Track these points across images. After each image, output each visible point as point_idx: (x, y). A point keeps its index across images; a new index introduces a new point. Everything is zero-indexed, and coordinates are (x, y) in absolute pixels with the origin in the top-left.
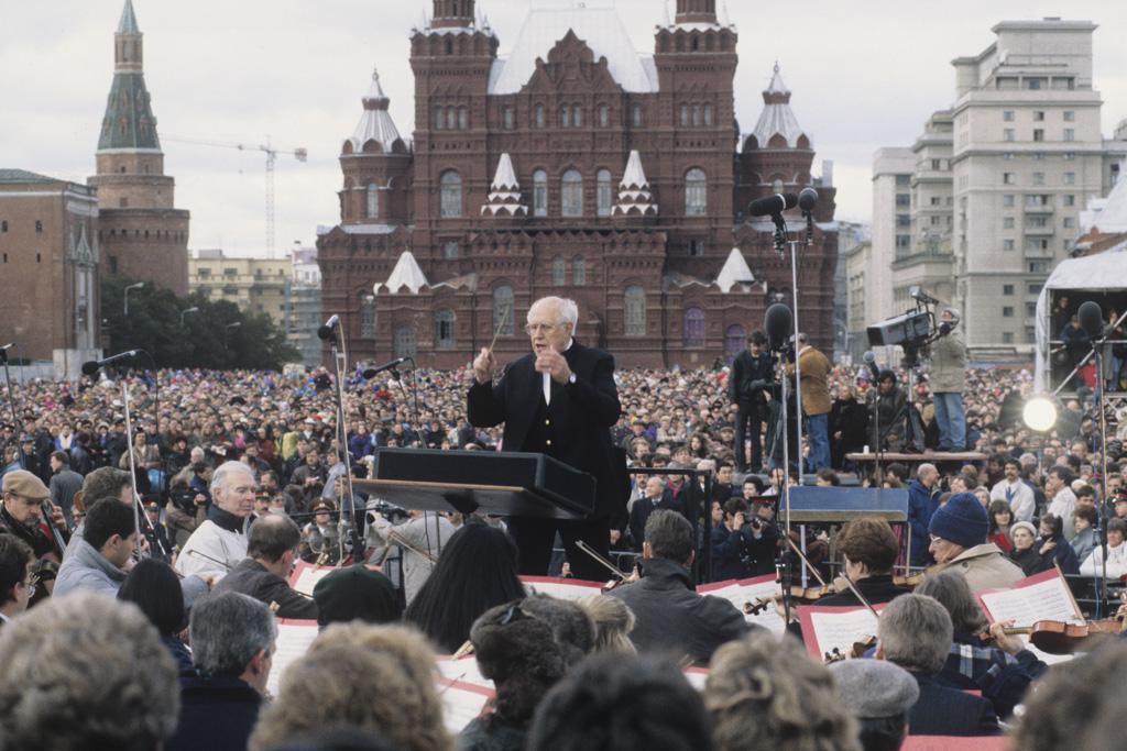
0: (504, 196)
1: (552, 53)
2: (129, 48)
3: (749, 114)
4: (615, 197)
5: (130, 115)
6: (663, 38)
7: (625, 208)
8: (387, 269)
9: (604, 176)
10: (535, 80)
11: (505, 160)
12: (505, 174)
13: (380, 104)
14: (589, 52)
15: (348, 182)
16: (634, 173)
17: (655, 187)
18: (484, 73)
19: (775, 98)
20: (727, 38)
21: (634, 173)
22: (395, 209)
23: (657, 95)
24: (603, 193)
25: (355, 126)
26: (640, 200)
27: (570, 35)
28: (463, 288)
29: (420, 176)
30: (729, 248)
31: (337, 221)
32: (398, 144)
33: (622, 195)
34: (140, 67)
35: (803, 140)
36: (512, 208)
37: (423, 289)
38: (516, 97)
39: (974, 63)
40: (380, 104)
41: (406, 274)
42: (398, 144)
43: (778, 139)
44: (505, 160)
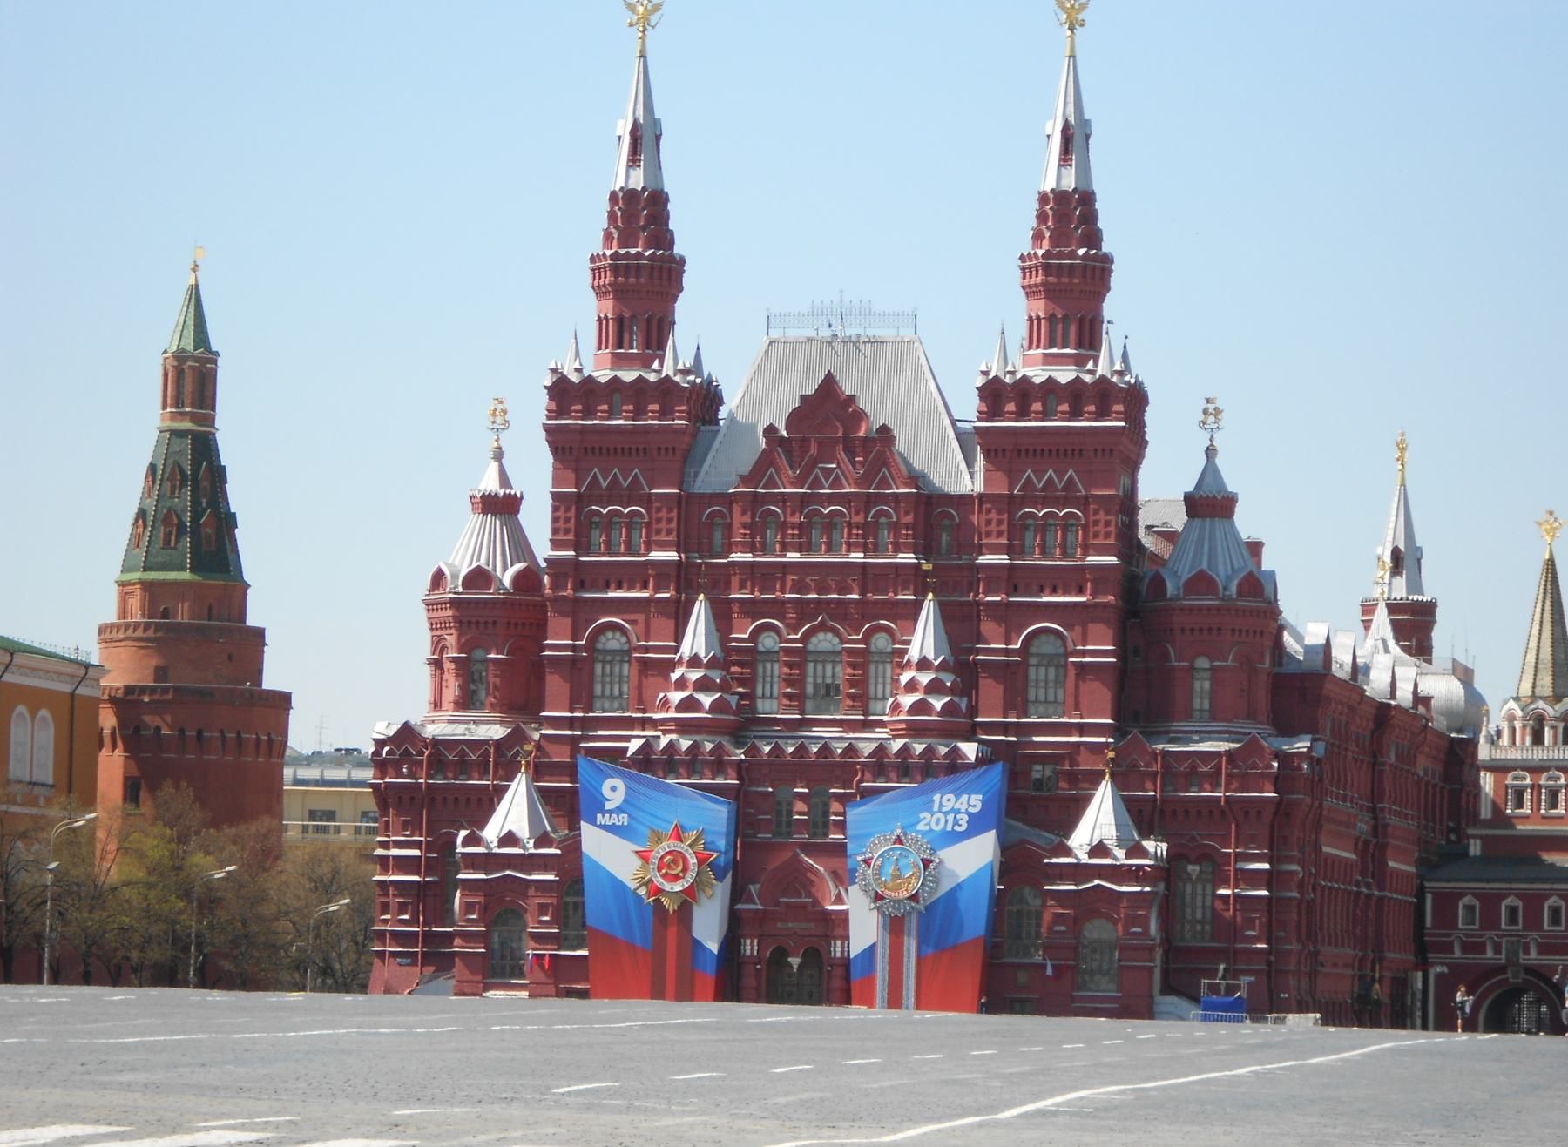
1: (794, 419)
2: (193, 380)
10: (765, 461)
13: (501, 506)
14: (860, 416)
19: (1211, 504)
23: (981, 496)
26: (934, 688)
27: (829, 382)
29: (558, 641)
34: (210, 420)
42: (527, 580)
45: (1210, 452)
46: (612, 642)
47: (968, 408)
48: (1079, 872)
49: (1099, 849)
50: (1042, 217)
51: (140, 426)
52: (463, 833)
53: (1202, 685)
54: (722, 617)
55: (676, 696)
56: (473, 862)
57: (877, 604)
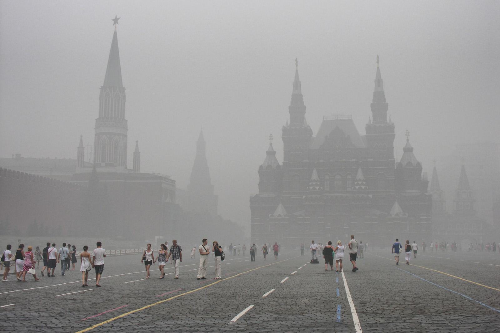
0: (314, 183)
3: (398, 155)
6: (369, 128)
7: (357, 187)
11: (315, 171)
12: (315, 176)
16: (360, 175)
19: (408, 150)
20: (391, 128)
21: (360, 175)
31: (258, 193)
33: (356, 183)
35: (419, 164)
36: (317, 188)
40: (271, 153)
41: (280, 211)
44: (315, 171)
45: (408, 140)
47: (362, 132)
52: (270, 215)
55: (311, 188)
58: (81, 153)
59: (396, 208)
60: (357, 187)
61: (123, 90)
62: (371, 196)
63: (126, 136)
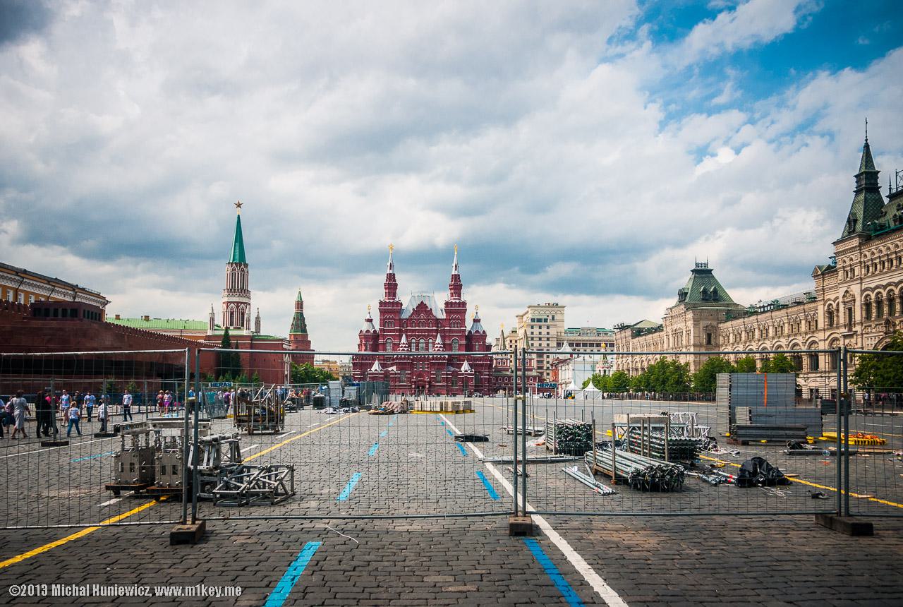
2: (300, 305)
3: (469, 325)
4: (434, 347)
5: (300, 323)
6: (447, 304)
7: (436, 349)
8: (371, 365)
9: (431, 341)
10: (413, 314)
11: (404, 335)
12: (404, 340)
13: (370, 321)
14: (427, 307)
15: (361, 341)
17: (444, 344)
18: (400, 312)
19: (476, 321)
20: (464, 304)
21: (439, 340)
22: (375, 347)
24: (430, 345)
25: (365, 327)
26: (440, 347)
28: (393, 370)
29: (381, 341)
30: (464, 361)
32: (375, 331)
35: (484, 332)
37: (381, 370)
38: (407, 319)
39: (522, 316)
40: (370, 321)
41: (376, 367)
42: (375, 331)
43: (477, 332)
44: (404, 335)
46: (389, 341)
48: (463, 374)
49: (466, 371)
50: (452, 278)
51: (293, 311)
53: (477, 347)
54: (407, 336)
55: (401, 349)
56: (370, 374)
57: (430, 335)
58: (212, 320)
59: (465, 367)
60: (436, 349)
61: (246, 265)
62: (447, 356)
63: (250, 304)
